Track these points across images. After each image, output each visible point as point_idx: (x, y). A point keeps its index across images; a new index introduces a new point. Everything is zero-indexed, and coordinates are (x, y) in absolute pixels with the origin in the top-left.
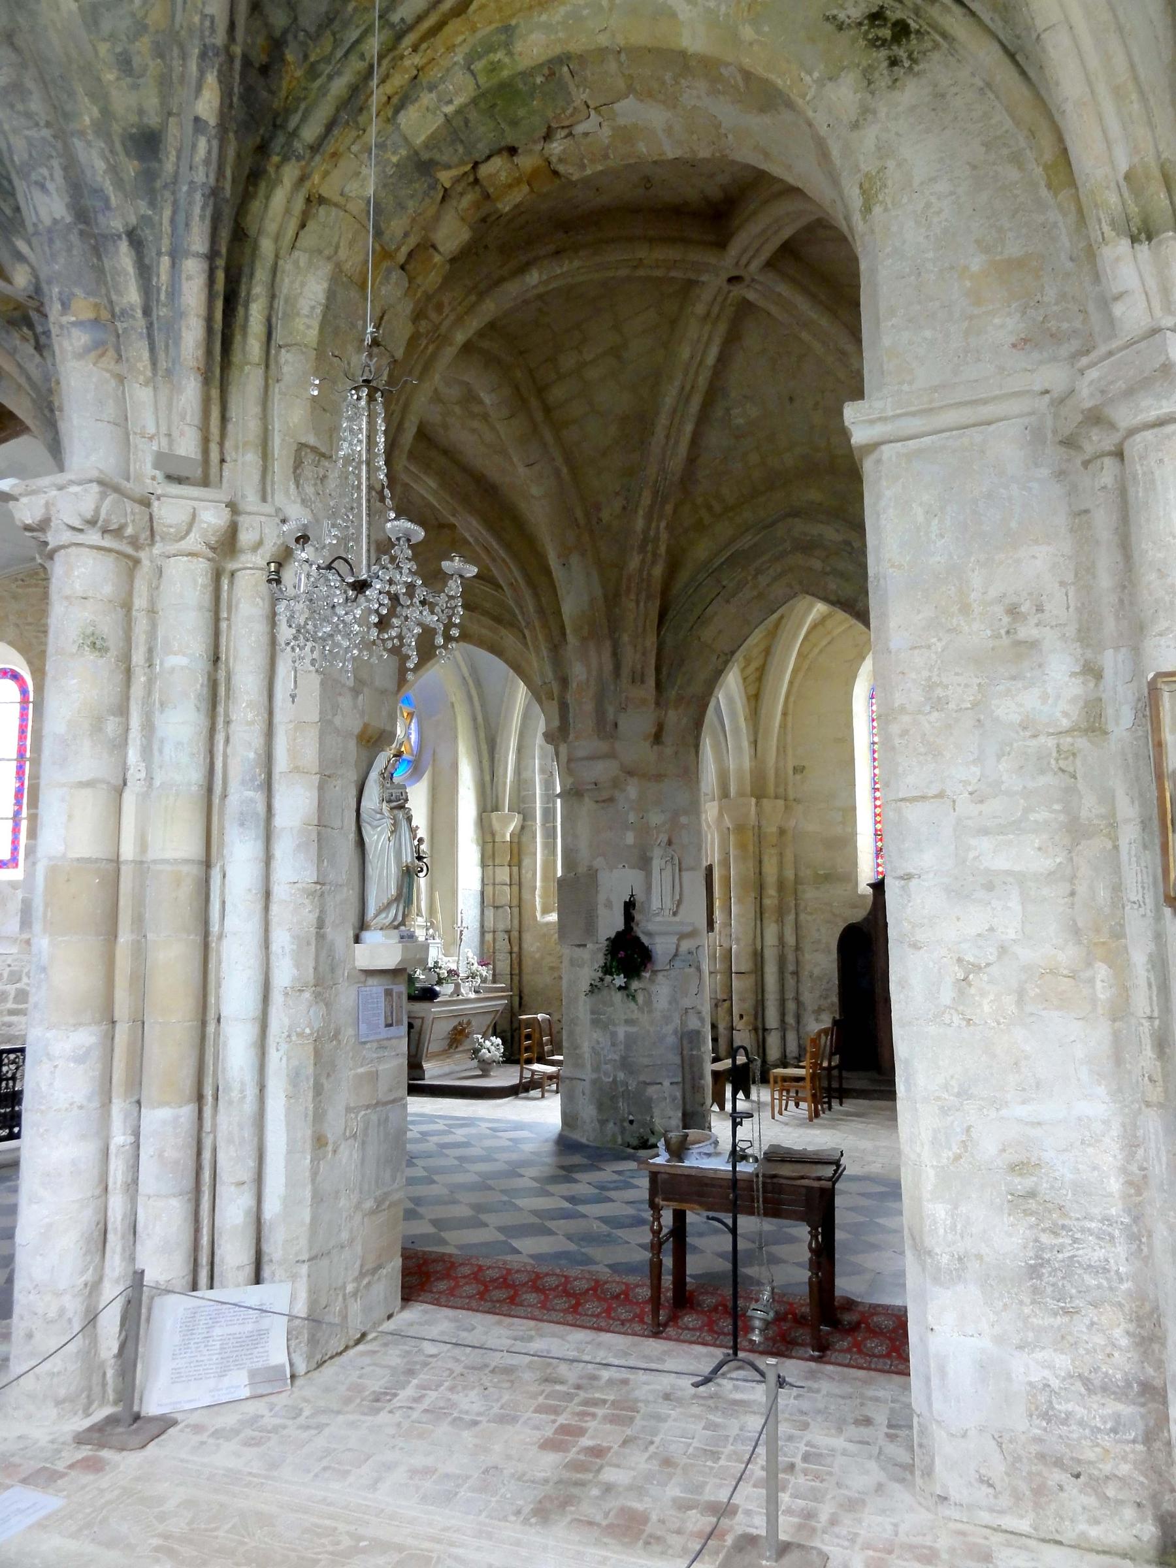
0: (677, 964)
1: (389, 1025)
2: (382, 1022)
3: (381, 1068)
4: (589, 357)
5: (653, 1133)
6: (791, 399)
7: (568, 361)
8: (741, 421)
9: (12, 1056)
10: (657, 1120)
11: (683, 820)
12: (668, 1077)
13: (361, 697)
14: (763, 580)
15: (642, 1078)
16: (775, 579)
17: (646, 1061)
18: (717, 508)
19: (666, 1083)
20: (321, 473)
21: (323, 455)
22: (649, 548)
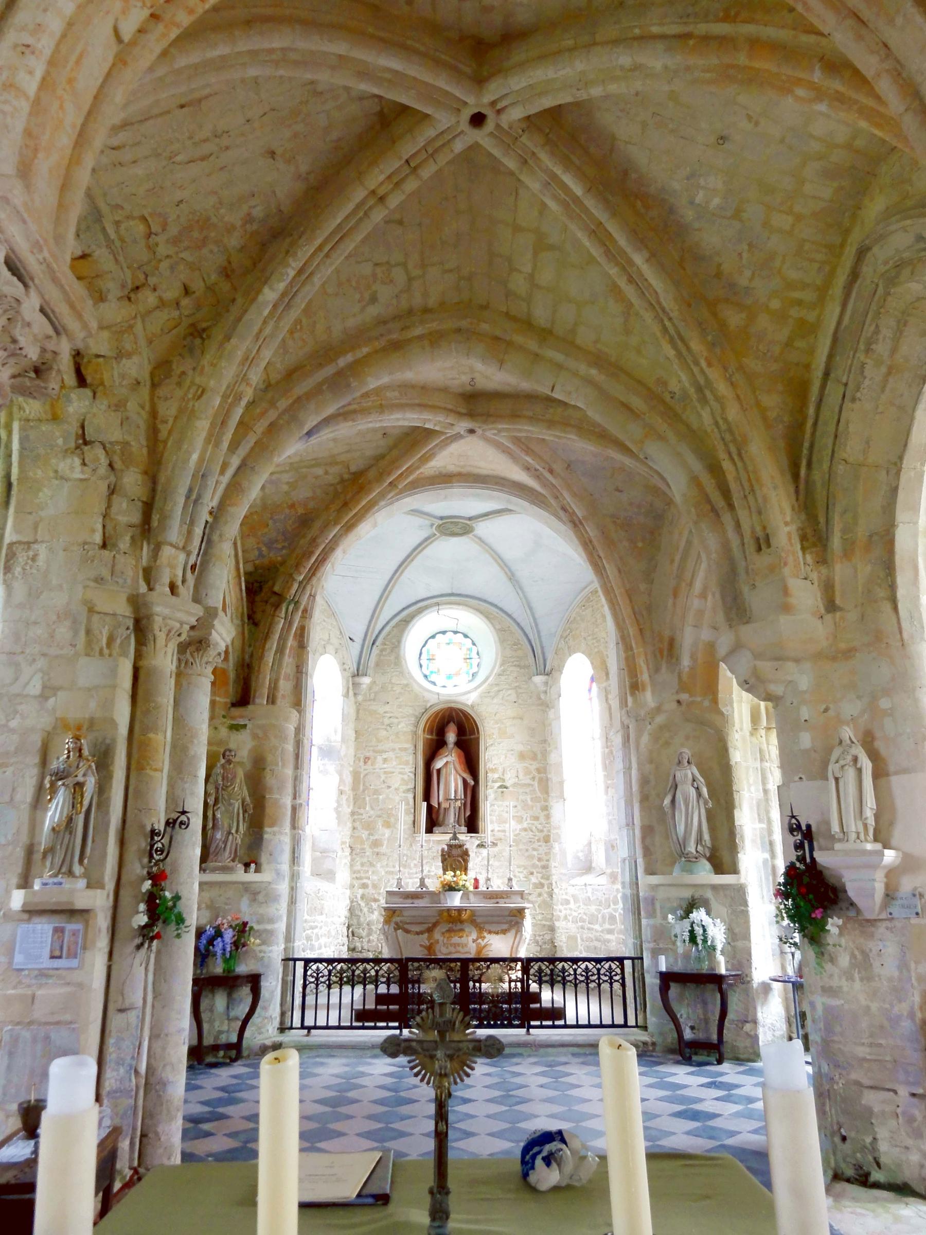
0: (896, 910)
1: (52, 957)
2: (46, 952)
3: (39, 993)
4: (528, 268)
5: (879, 1165)
6: (723, 139)
7: (519, 284)
8: (716, 201)
9: (416, 964)
10: (883, 1147)
11: (884, 704)
12: (908, 1083)
13: (52, 701)
14: (882, 348)
15: (854, 1076)
16: (899, 333)
17: (862, 1051)
18: (808, 296)
19: (903, 1092)
20: (31, 553)
21: (28, 543)
22: (708, 393)
